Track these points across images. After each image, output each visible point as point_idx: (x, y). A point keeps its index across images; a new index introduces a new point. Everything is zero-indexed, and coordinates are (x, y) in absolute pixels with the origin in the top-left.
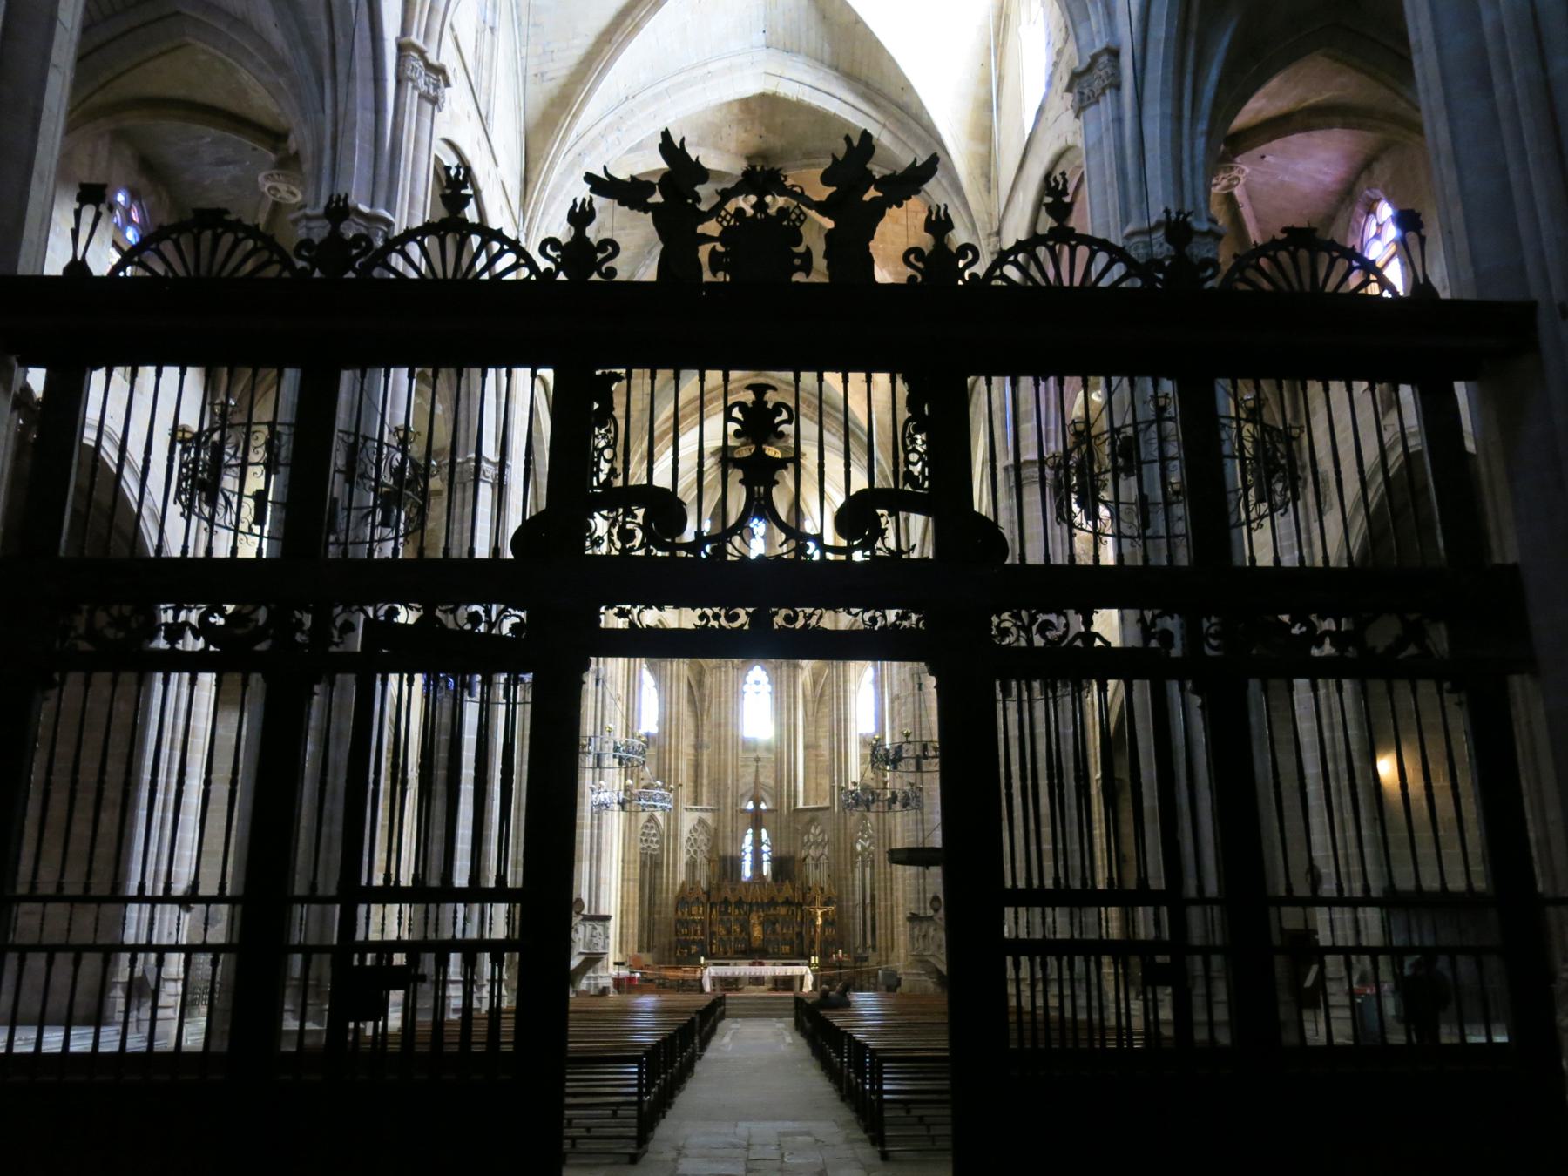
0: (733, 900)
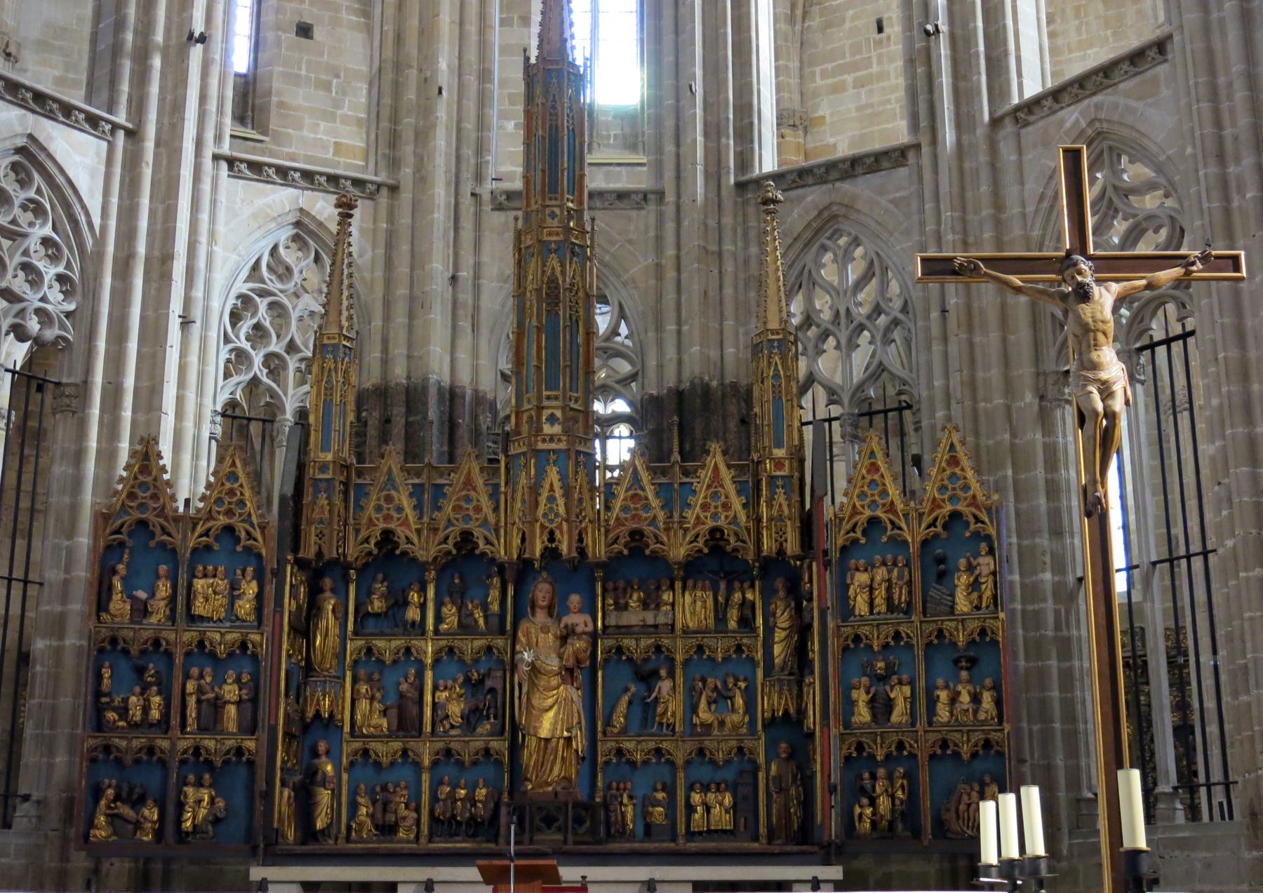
0: (426, 550)
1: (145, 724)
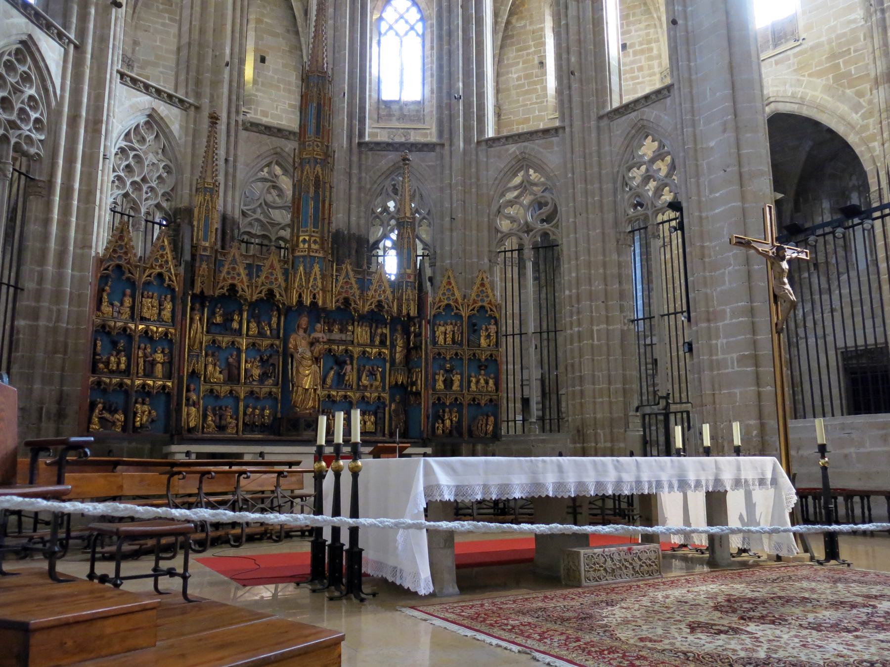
1: (118, 372)
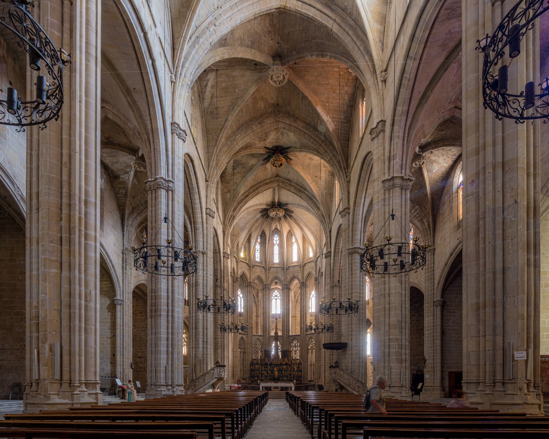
0: (269, 363)
